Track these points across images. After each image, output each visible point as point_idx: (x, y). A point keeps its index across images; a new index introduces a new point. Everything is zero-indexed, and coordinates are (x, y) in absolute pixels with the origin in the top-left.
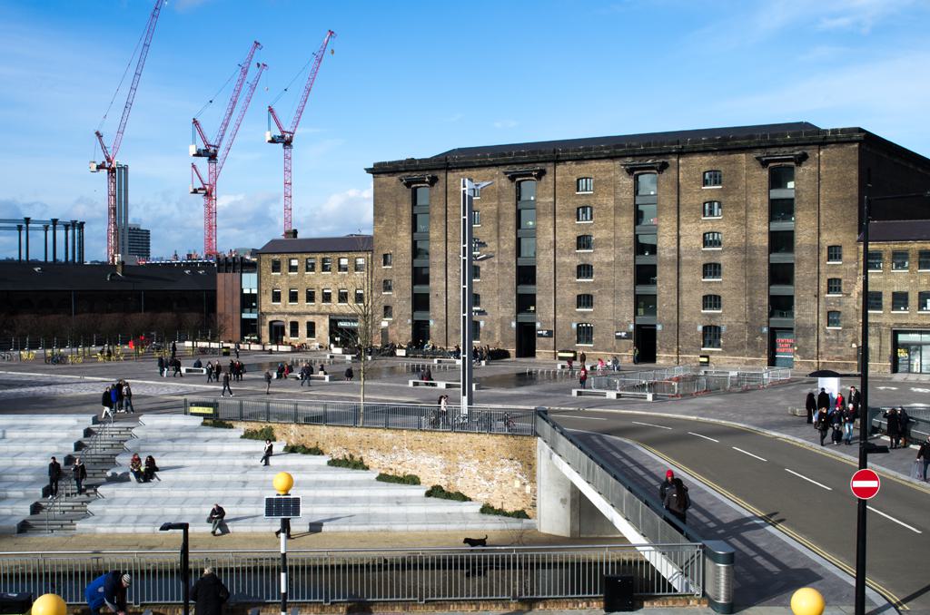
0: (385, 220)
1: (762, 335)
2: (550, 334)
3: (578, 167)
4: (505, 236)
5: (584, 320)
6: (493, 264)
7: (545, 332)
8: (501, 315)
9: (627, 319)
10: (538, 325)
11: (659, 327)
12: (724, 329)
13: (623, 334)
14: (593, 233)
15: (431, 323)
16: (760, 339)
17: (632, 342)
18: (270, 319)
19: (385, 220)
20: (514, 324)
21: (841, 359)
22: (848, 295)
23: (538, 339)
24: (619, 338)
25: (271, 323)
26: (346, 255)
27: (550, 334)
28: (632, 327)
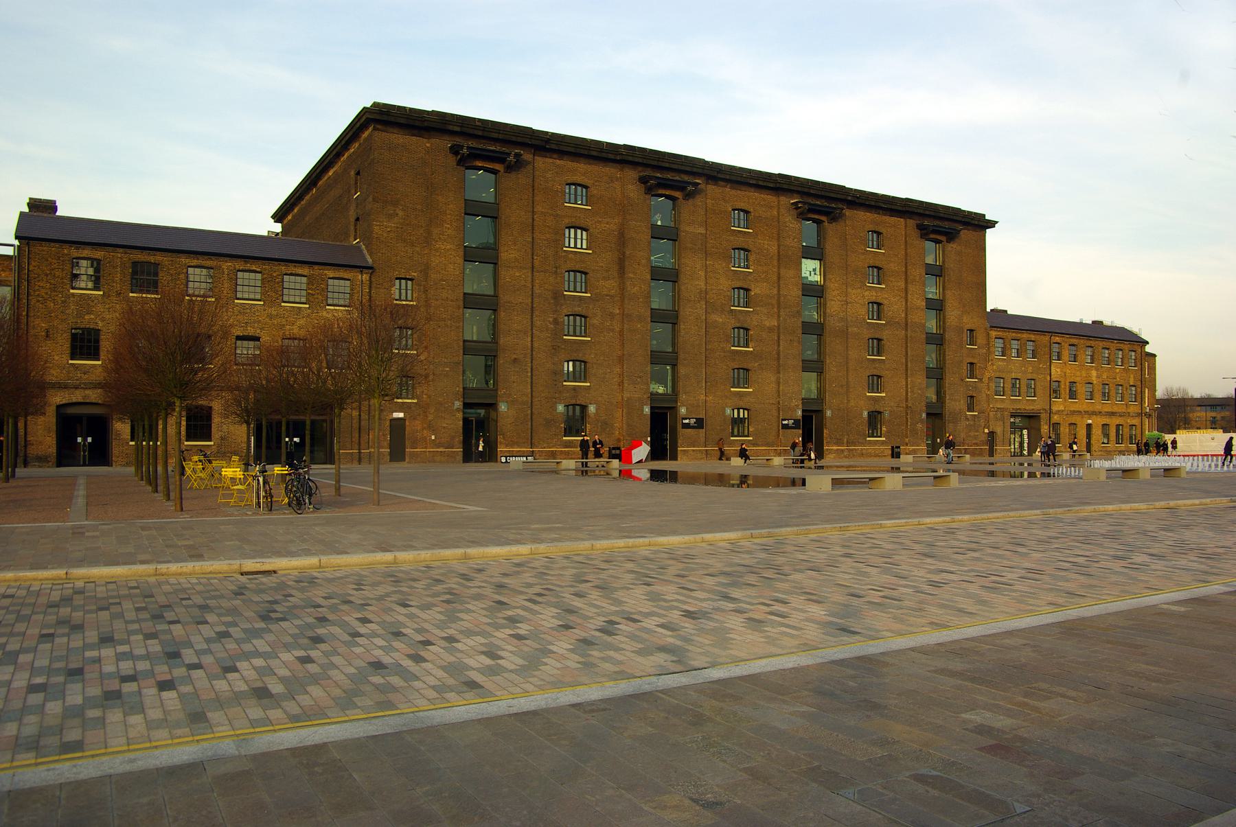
0: (401, 213)
1: (921, 421)
2: (700, 423)
3: (733, 192)
4: (635, 273)
5: (742, 404)
6: (612, 315)
7: (693, 421)
8: (626, 395)
9: (794, 403)
10: (683, 410)
11: (829, 413)
12: (886, 415)
13: (791, 422)
14: (752, 287)
15: (503, 407)
16: (919, 425)
17: (801, 431)
18: (58, 398)
19: (401, 213)
20: (647, 410)
21: (976, 444)
22: (981, 380)
23: (682, 432)
24: (785, 427)
25: (59, 407)
26: (305, 270)
27: (700, 423)
28: (800, 413)
